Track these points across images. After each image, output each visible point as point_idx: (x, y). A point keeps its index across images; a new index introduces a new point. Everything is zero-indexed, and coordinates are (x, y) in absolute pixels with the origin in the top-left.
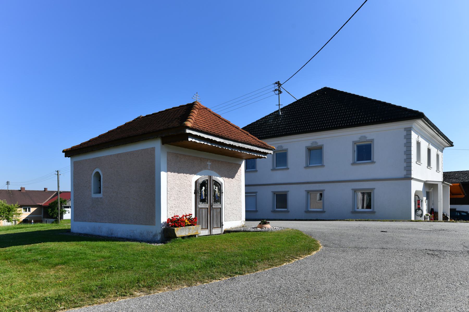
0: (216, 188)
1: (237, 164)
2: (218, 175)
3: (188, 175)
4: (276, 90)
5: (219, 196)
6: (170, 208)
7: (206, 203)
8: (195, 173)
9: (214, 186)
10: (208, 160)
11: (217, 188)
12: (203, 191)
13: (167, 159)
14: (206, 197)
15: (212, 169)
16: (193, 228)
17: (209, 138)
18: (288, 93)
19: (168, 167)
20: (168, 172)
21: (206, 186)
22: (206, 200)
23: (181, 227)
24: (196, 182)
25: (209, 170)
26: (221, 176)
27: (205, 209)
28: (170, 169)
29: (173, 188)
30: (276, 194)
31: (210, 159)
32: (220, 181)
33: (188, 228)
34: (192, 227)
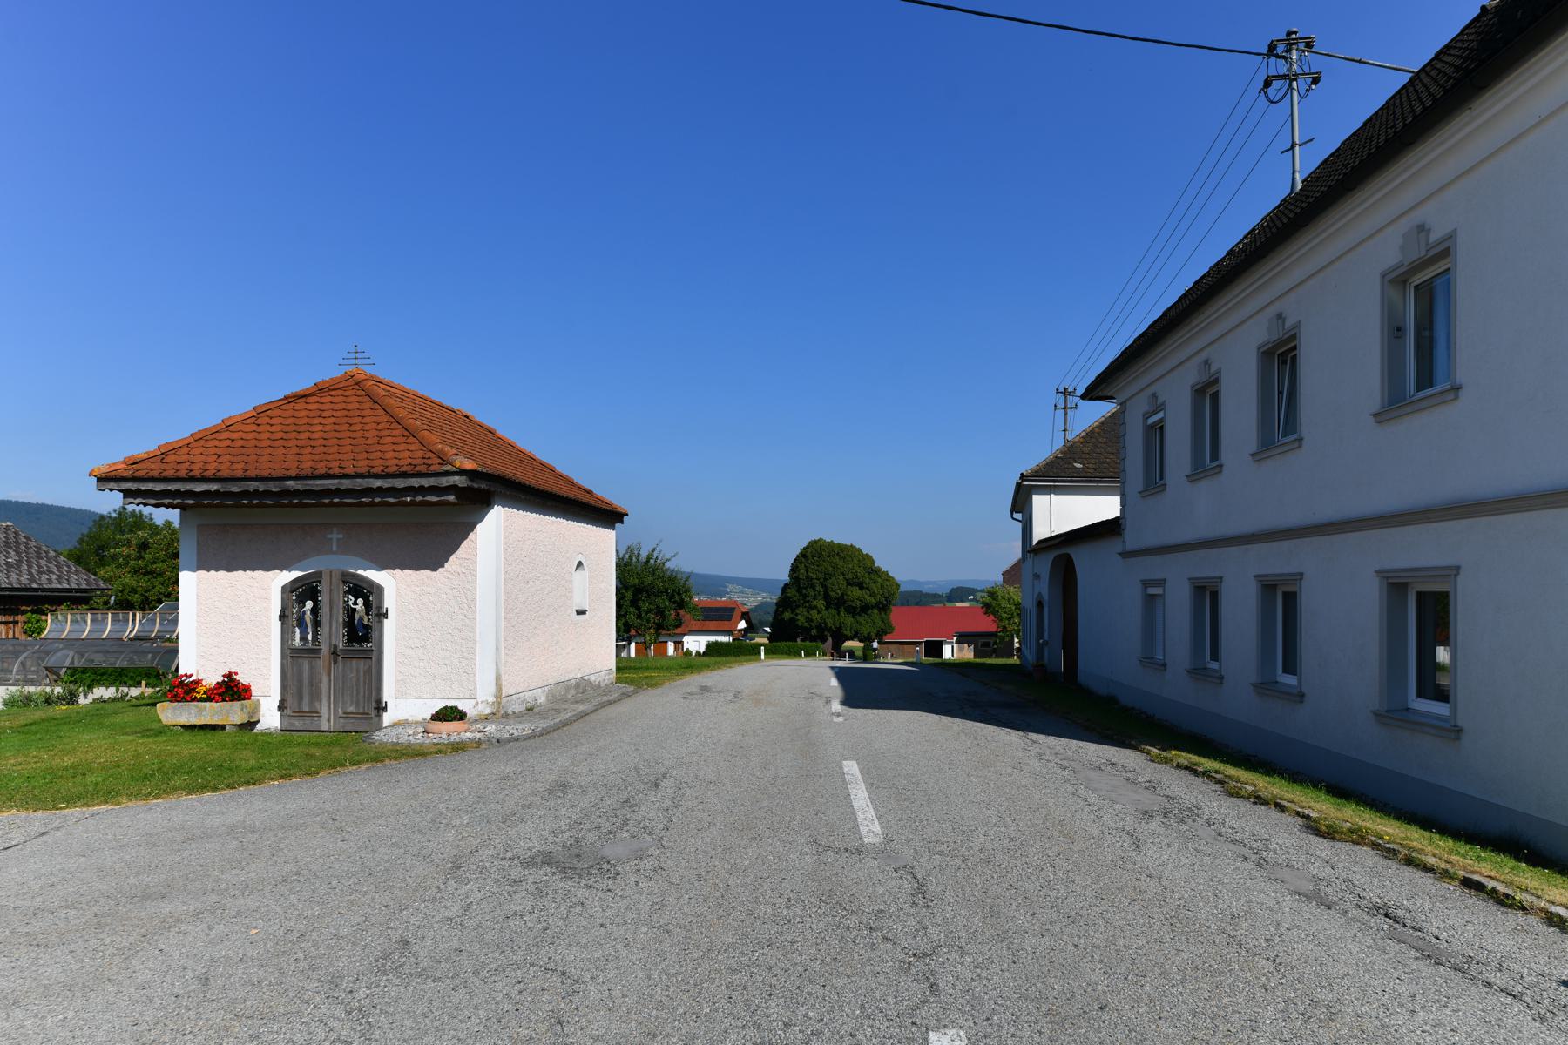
0: (355, 603)
2: (368, 563)
3: (259, 574)
4: (1267, 84)
9: (351, 597)
11: (360, 601)
12: (309, 613)
13: (198, 541)
15: (344, 549)
16: (211, 706)
17: (169, 488)
18: (1360, 61)
19: (198, 560)
26: (382, 566)
28: (204, 564)
30: (1211, 592)
31: (335, 524)
33: (196, 706)
34: (208, 704)
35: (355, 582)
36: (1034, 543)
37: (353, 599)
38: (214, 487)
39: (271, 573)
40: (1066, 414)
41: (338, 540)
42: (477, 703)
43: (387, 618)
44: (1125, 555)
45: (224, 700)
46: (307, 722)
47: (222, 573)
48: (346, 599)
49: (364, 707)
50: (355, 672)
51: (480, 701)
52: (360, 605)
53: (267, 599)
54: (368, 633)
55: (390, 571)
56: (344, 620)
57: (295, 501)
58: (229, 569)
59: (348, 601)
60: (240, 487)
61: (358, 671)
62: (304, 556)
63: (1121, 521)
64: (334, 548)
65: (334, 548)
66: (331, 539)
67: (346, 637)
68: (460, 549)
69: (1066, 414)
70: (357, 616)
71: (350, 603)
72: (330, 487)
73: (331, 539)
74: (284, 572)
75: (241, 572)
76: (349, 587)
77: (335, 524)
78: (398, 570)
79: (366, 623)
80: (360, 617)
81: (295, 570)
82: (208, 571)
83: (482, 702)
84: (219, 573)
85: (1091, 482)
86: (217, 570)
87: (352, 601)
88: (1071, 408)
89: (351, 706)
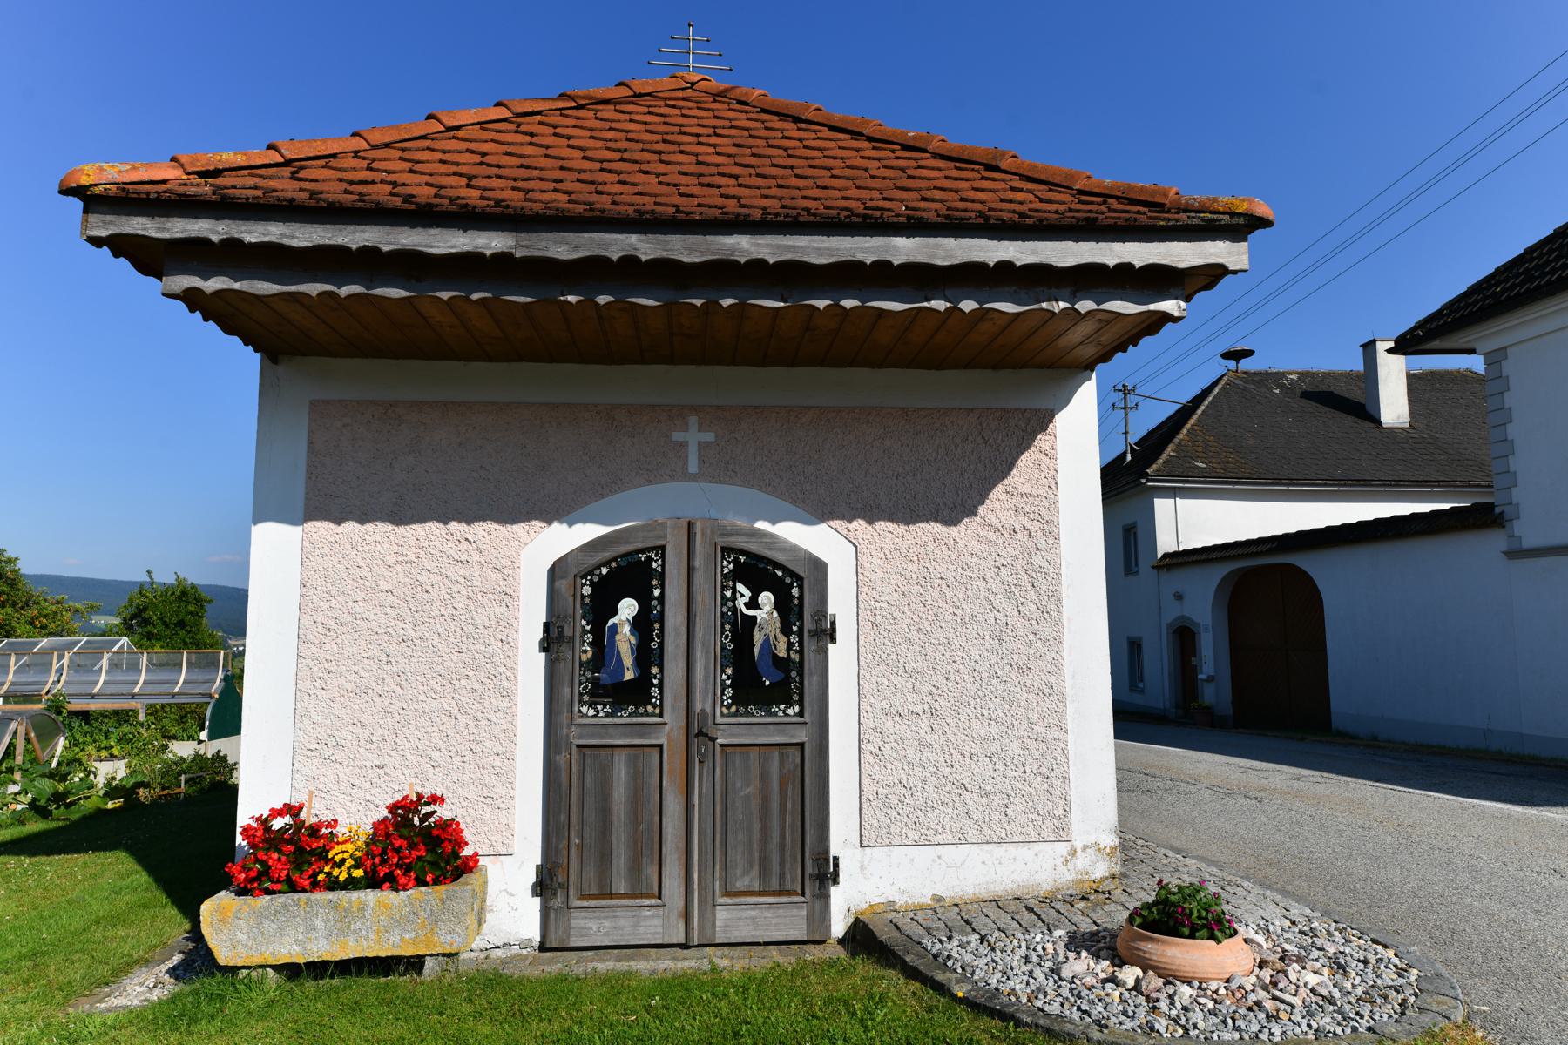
0: (753, 604)
1: (1009, 411)
3: (482, 530)
5: (794, 656)
6: (313, 746)
7: (647, 714)
8: (552, 511)
9: (741, 587)
10: (678, 414)
11: (766, 598)
12: (626, 629)
14: (654, 670)
15: (719, 468)
16: (379, 904)
20: (310, 525)
21: (657, 592)
22: (654, 691)
23: (268, 897)
24: (555, 572)
25: (693, 478)
26: (819, 512)
27: (627, 751)
29: (347, 618)
32: (795, 549)
33: (335, 906)
34: (370, 896)
35: (753, 547)
36: (1159, 557)
37: (748, 593)
38: (492, 242)
39: (519, 529)
40: (1126, 415)
41: (703, 446)
42: (1073, 853)
43: (833, 640)
44: (1516, 554)
45: (421, 882)
46: (622, 922)
47: (379, 530)
48: (728, 594)
49: (782, 876)
50: (756, 783)
51: (1079, 845)
52: (767, 608)
53: (508, 596)
54: (787, 680)
55: (840, 524)
56: (723, 648)
57: (727, 302)
58: (400, 516)
59: (734, 599)
60: (576, 248)
61: (764, 777)
62: (614, 484)
63: (1497, 510)
64: (693, 467)
65: (693, 467)
66: (684, 444)
67: (729, 692)
68: (1015, 471)
69: (1126, 415)
70: (758, 638)
71: (741, 603)
72: (860, 257)
73: (684, 444)
74: (556, 525)
75: (433, 527)
76: (736, 561)
77: (695, 409)
78: (859, 524)
79: (782, 653)
80: (767, 640)
81: (585, 521)
82: (338, 521)
83: (1085, 848)
84: (369, 527)
85: (1226, 483)
86: (362, 521)
87: (746, 599)
88: (1131, 408)
89: (746, 872)
